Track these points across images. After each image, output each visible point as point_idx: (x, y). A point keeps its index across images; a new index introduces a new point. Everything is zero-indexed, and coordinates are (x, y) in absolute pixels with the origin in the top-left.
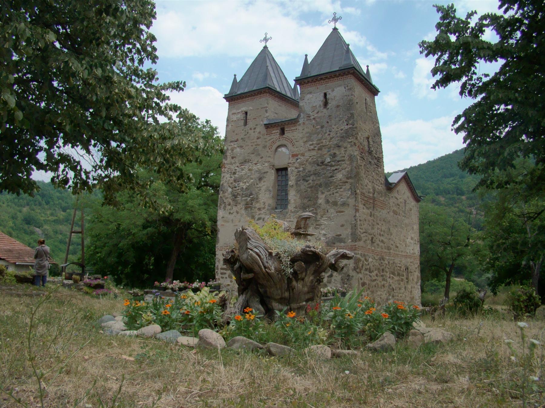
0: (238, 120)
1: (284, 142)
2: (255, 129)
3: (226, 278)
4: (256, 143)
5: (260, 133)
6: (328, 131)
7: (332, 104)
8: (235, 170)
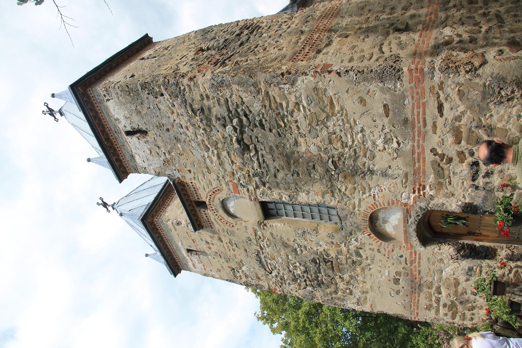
0: (202, 262)
1: (217, 202)
4: (230, 245)
6: (181, 131)
7: (137, 122)
8: (276, 276)
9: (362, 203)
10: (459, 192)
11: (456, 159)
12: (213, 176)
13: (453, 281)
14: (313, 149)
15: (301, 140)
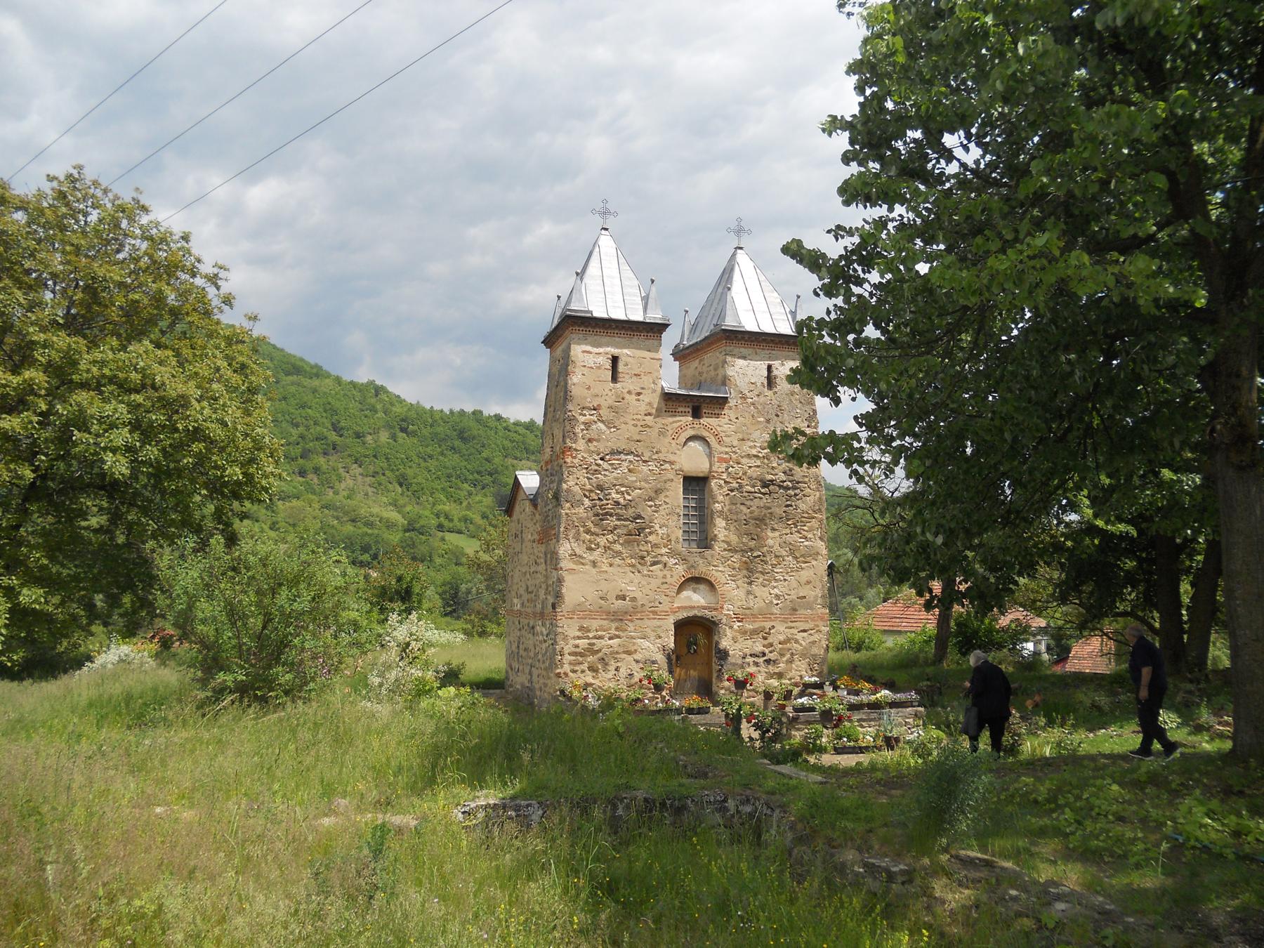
0: (599, 368)
1: (705, 434)
2: (639, 394)
3: (583, 672)
5: (650, 404)
8: (598, 465)
9: (719, 573)
10: (738, 646)
11: (766, 642)
12: (735, 443)
13: (633, 649)
14: (770, 542)
15: (777, 534)
